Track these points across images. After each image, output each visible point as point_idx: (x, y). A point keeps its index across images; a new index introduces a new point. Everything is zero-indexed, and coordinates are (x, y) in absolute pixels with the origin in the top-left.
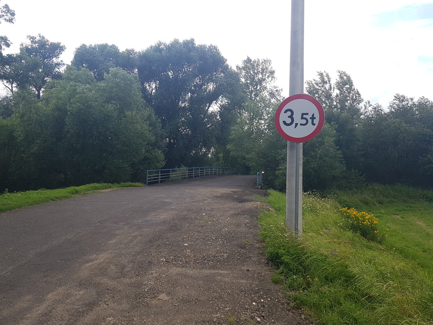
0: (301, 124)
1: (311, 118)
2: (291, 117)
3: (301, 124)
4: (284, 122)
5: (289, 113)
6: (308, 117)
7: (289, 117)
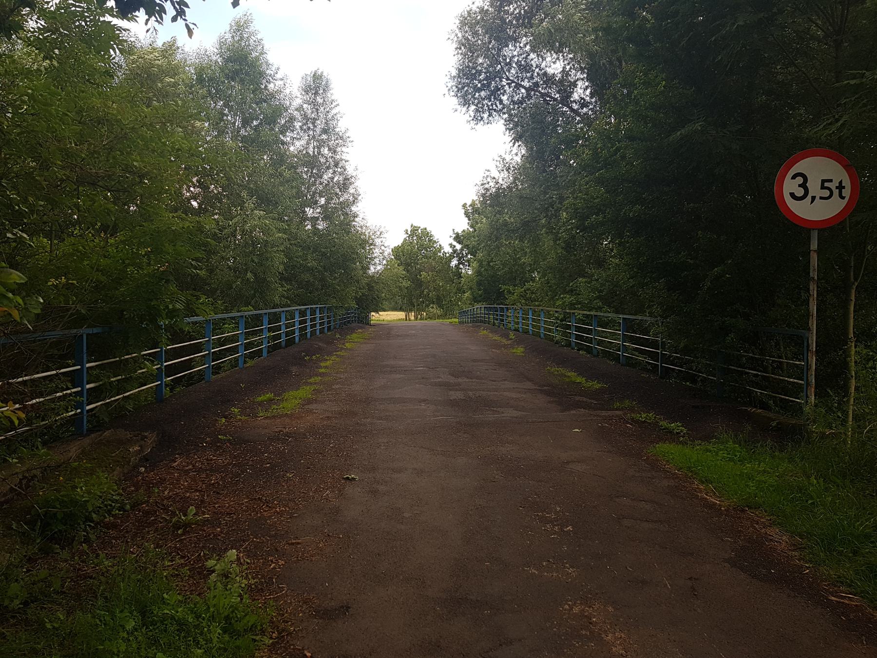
0: (821, 198)
1: (837, 188)
2: (804, 185)
3: (821, 198)
4: (792, 195)
5: (800, 180)
6: (833, 186)
7: (800, 186)
